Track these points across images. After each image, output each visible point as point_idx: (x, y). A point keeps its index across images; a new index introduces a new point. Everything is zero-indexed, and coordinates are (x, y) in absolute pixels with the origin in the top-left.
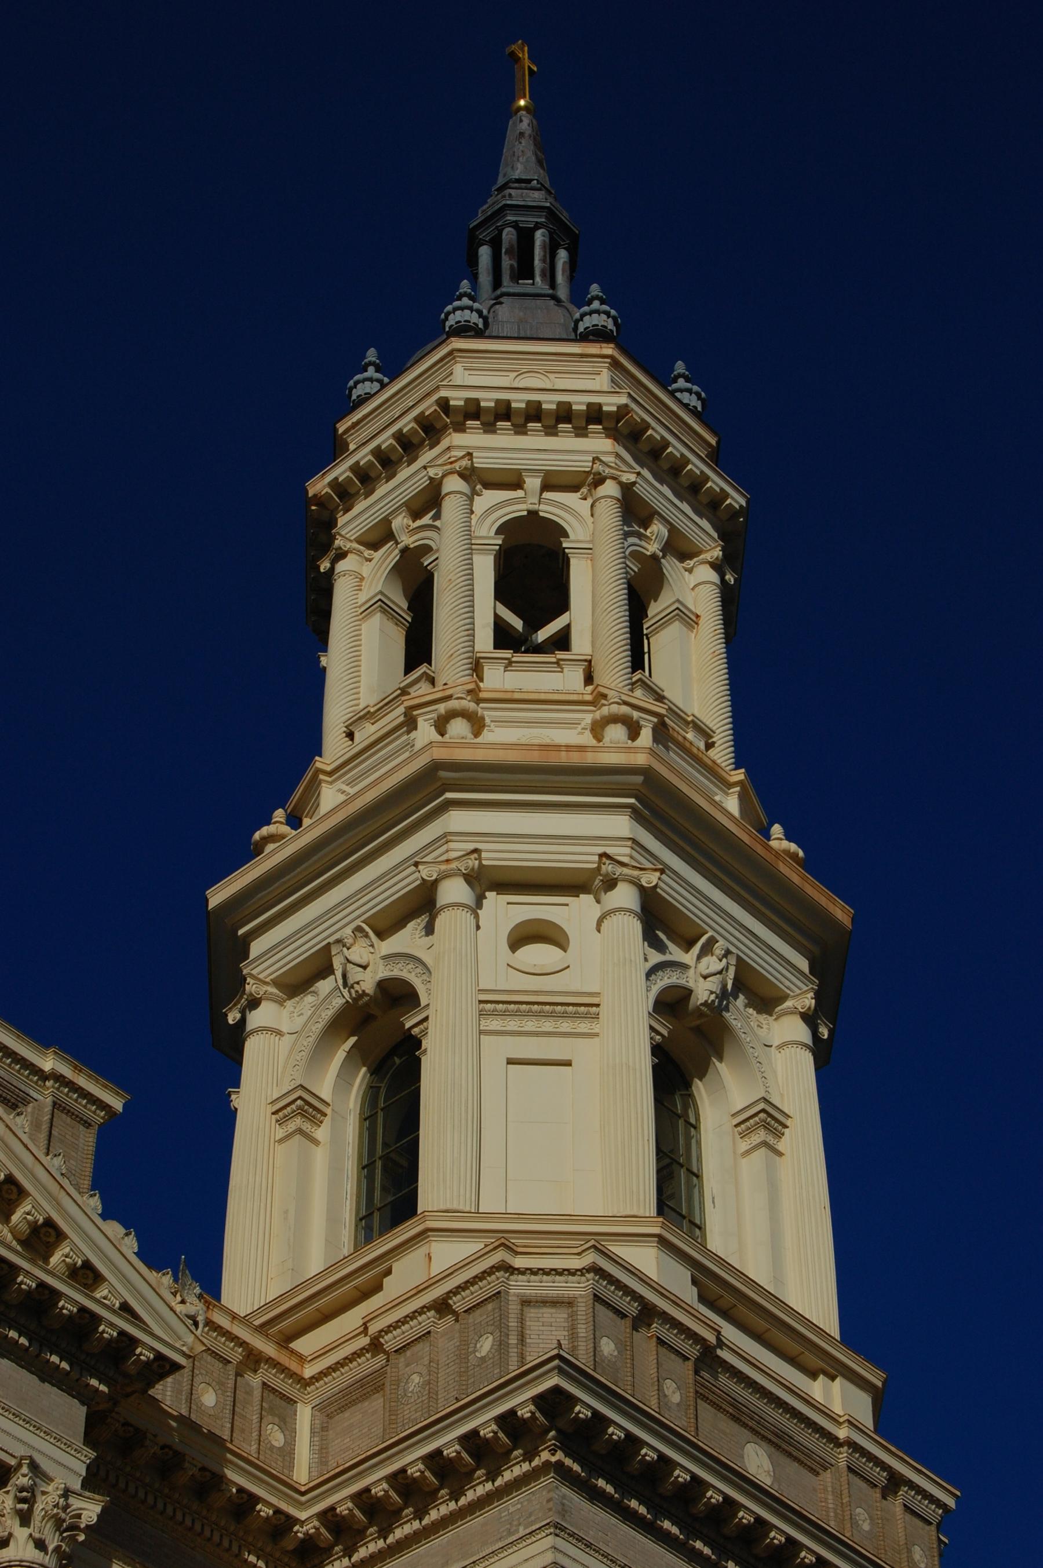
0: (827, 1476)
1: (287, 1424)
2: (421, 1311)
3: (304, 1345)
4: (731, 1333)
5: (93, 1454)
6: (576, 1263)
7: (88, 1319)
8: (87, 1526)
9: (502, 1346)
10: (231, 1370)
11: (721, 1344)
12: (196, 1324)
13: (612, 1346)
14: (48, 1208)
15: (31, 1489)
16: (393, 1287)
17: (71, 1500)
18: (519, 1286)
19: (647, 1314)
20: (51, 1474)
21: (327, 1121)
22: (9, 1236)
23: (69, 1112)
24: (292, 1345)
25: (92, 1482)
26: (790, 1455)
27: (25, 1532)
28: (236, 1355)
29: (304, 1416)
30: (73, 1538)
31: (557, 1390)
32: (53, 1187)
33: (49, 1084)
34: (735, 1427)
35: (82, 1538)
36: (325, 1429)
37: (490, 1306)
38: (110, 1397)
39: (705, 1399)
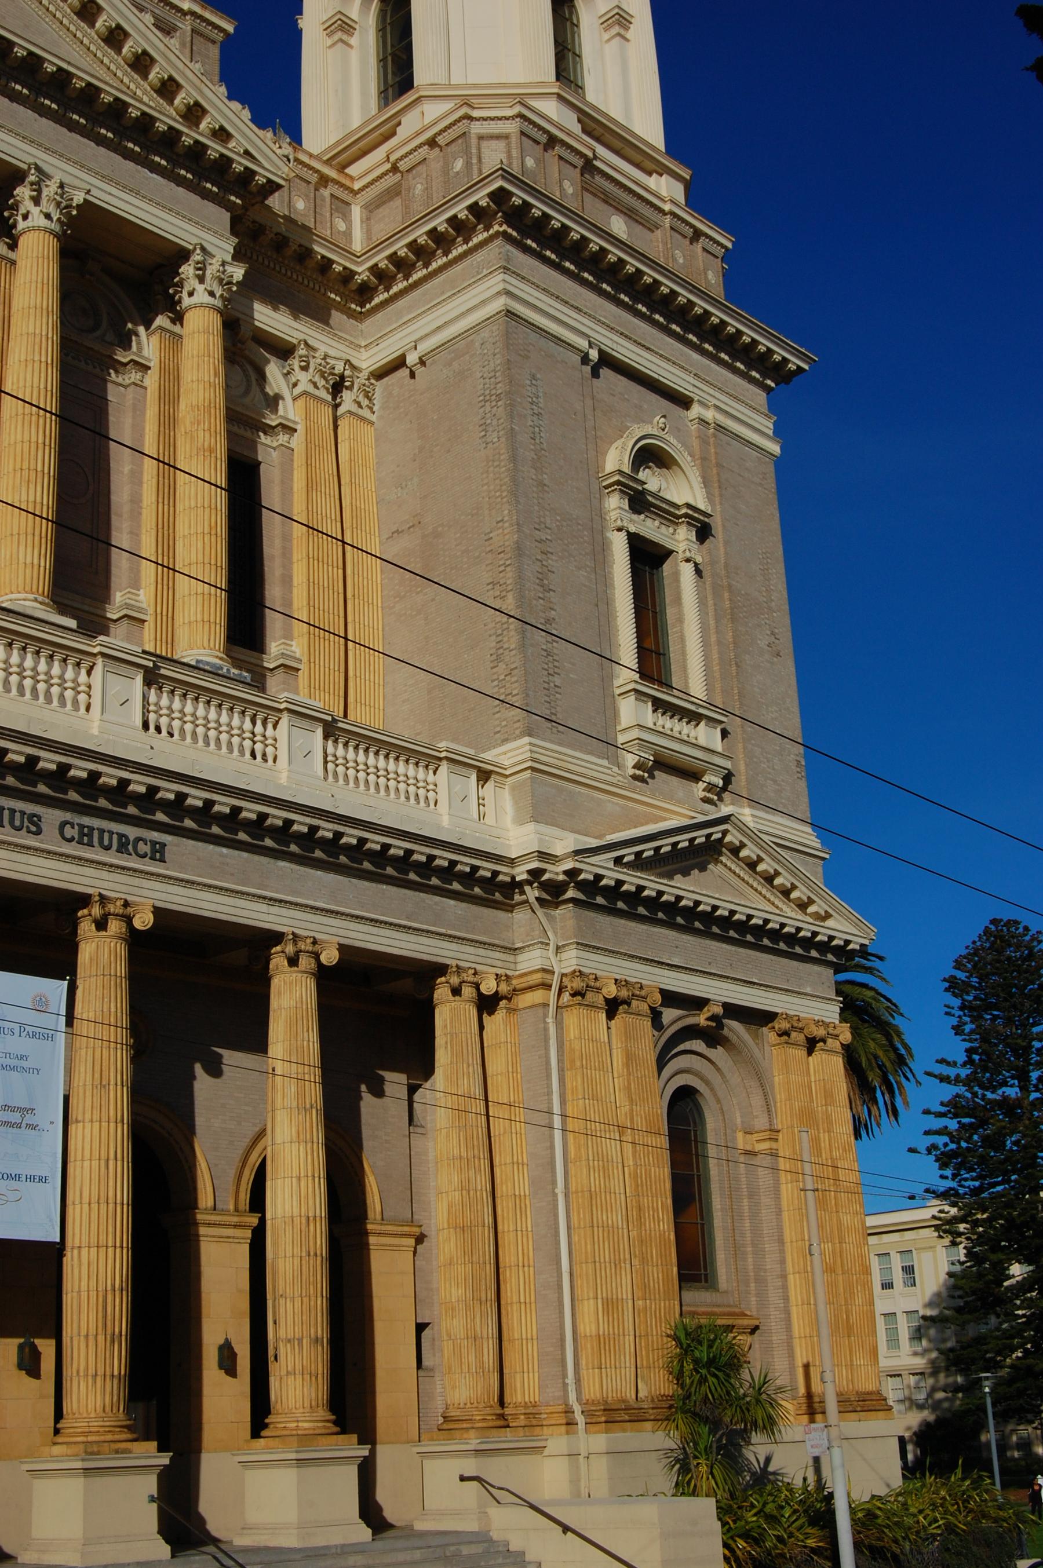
0: (658, 233)
1: (346, 217)
2: (420, 146)
3: (353, 170)
4: (601, 150)
5: (237, 240)
6: (509, 113)
7: (225, 161)
9: (468, 164)
10: (312, 188)
11: (595, 157)
12: (289, 160)
13: (532, 161)
14: (195, 95)
15: (203, 262)
16: (403, 133)
17: (226, 268)
18: (476, 128)
19: (552, 141)
20: (214, 253)
21: (357, 33)
23: (201, 35)
24: (347, 171)
25: (238, 255)
26: (637, 221)
28: (314, 178)
29: (356, 212)
30: (230, 289)
31: (501, 189)
33: (188, 17)
35: (235, 289)
36: (368, 219)
37: (460, 141)
38: (245, 207)
39: (587, 190)
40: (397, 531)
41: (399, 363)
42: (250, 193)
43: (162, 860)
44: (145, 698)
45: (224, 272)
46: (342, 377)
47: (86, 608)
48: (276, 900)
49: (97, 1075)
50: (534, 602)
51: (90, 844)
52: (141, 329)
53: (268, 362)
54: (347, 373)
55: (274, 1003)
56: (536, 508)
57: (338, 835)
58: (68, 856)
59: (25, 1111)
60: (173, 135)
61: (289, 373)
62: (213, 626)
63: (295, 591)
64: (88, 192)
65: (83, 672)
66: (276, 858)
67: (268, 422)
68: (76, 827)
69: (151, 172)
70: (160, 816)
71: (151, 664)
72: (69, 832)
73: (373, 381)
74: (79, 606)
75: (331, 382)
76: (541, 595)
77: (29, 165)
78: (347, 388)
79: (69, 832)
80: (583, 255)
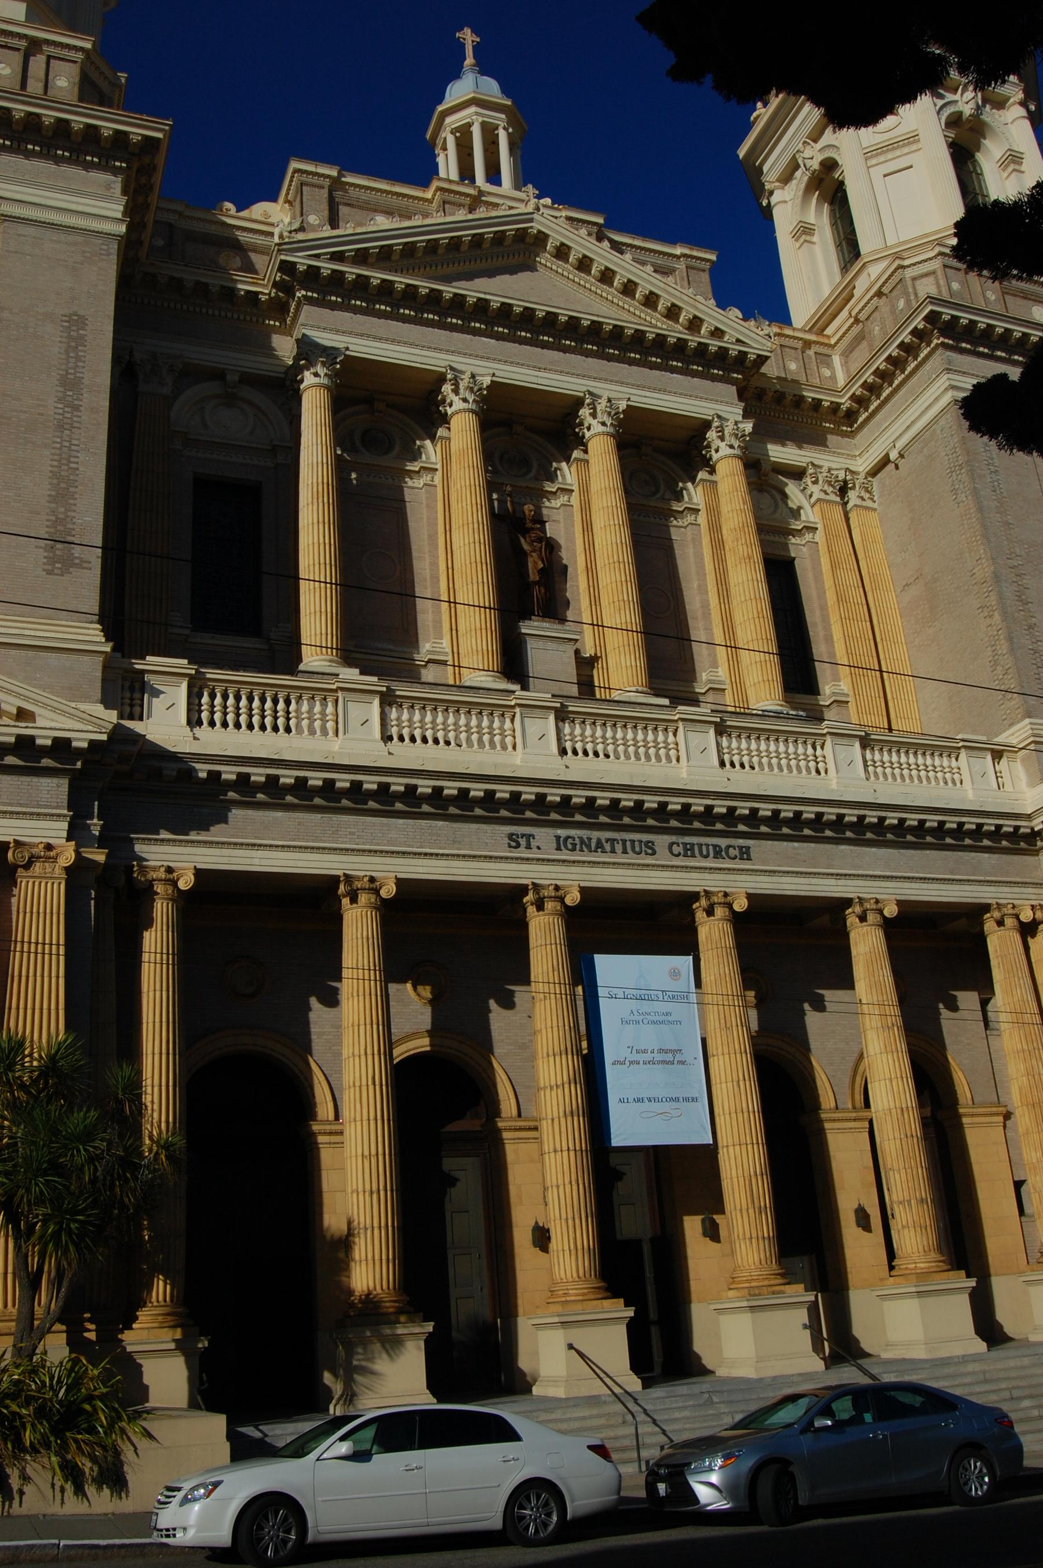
1: (830, 366)
3: (828, 331)
5: (743, 404)
6: (932, 254)
7: (723, 352)
8: (487, 387)
9: (908, 302)
10: (799, 351)
12: (770, 337)
13: (957, 284)
14: (692, 311)
15: (721, 426)
16: (857, 293)
17: (739, 425)
20: (727, 417)
22: (681, 328)
23: (694, 268)
24: (825, 333)
25: (746, 415)
27: (724, 443)
28: (800, 345)
29: (837, 360)
30: (744, 440)
31: (932, 312)
32: (692, 301)
33: (682, 259)
34: (1025, 301)
35: (748, 439)
36: (846, 363)
37: (899, 286)
38: (744, 379)
40: (907, 585)
41: (885, 461)
42: (748, 368)
43: (749, 859)
44: (559, 732)
45: (738, 428)
46: (845, 482)
47: (681, 689)
48: (841, 875)
49: (723, 1021)
50: (1016, 614)
51: (693, 856)
52: (689, 485)
53: (787, 484)
54: (848, 478)
55: (854, 952)
56: (1006, 543)
57: (882, 820)
58: (677, 867)
59: (674, 1052)
60: (682, 343)
61: (805, 489)
62: (771, 683)
63: (836, 645)
64: (629, 399)
65: (671, 734)
66: (837, 844)
67: (793, 527)
68: (681, 845)
69: (672, 373)
70: (741, 828)
71: (718, 720)
72: (676, 849)
73: (869, 479)
74: (676, 688)
75: (838, 487)
76: (1021, 608)
77: (584, 392)
78: (851, 489)
79: (676, 849)
80: (1010, 343)
